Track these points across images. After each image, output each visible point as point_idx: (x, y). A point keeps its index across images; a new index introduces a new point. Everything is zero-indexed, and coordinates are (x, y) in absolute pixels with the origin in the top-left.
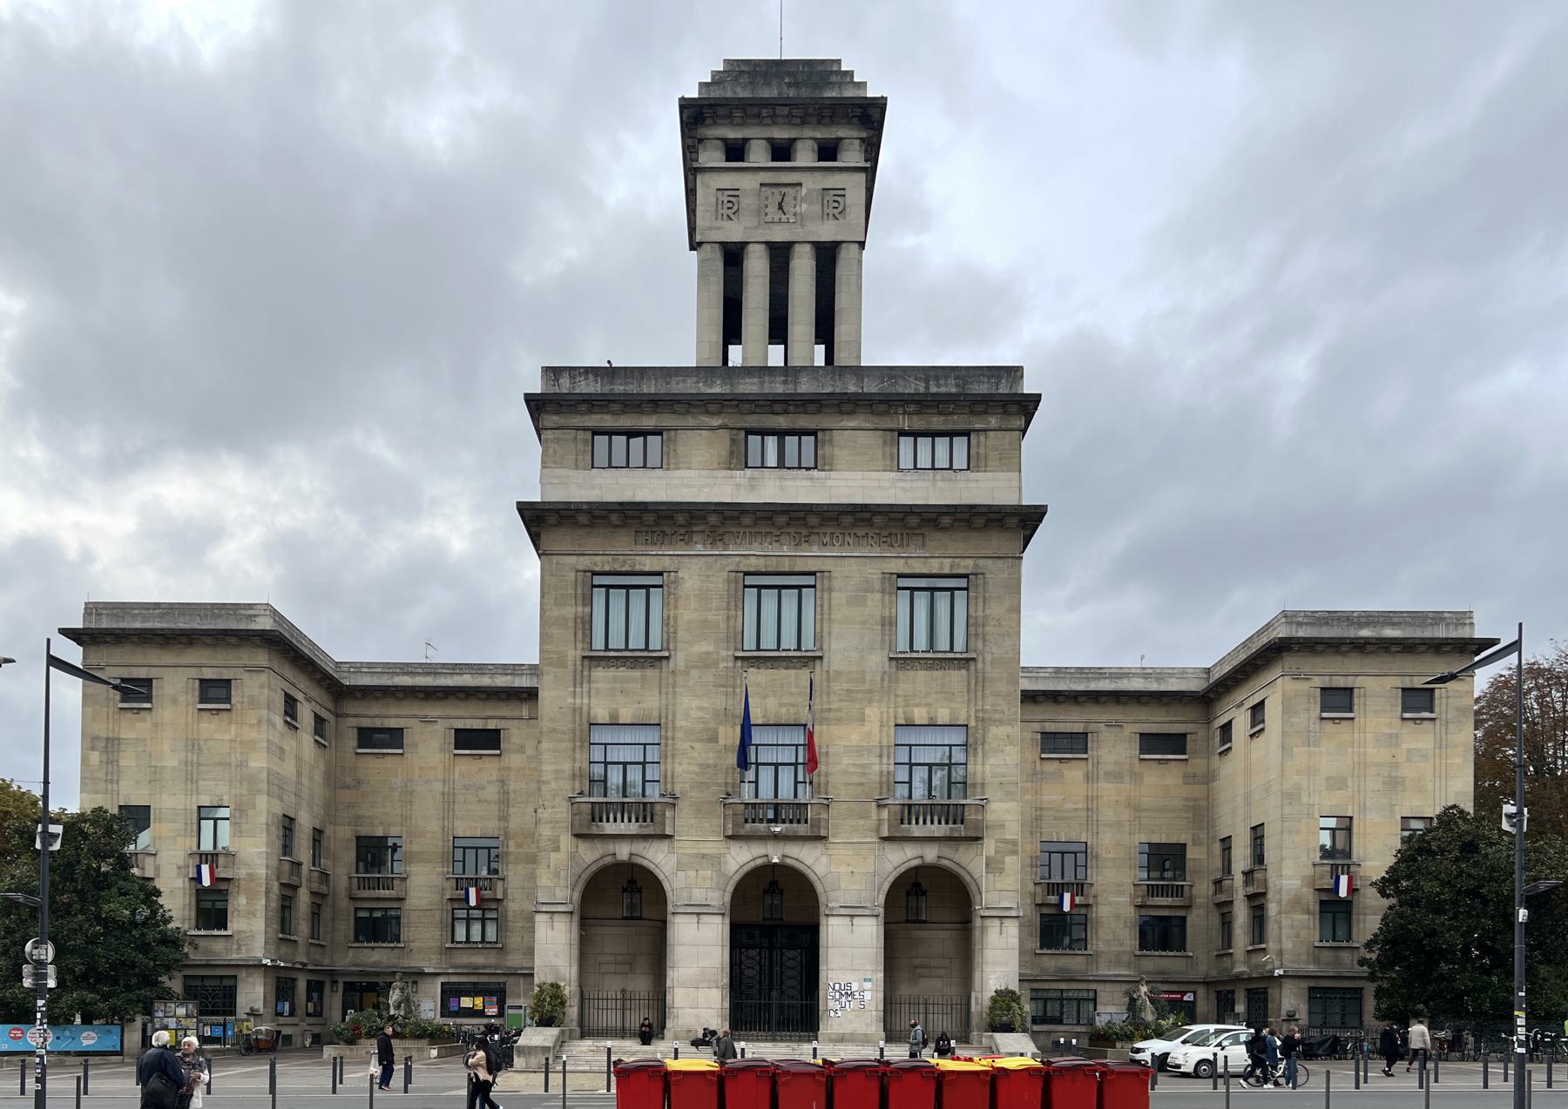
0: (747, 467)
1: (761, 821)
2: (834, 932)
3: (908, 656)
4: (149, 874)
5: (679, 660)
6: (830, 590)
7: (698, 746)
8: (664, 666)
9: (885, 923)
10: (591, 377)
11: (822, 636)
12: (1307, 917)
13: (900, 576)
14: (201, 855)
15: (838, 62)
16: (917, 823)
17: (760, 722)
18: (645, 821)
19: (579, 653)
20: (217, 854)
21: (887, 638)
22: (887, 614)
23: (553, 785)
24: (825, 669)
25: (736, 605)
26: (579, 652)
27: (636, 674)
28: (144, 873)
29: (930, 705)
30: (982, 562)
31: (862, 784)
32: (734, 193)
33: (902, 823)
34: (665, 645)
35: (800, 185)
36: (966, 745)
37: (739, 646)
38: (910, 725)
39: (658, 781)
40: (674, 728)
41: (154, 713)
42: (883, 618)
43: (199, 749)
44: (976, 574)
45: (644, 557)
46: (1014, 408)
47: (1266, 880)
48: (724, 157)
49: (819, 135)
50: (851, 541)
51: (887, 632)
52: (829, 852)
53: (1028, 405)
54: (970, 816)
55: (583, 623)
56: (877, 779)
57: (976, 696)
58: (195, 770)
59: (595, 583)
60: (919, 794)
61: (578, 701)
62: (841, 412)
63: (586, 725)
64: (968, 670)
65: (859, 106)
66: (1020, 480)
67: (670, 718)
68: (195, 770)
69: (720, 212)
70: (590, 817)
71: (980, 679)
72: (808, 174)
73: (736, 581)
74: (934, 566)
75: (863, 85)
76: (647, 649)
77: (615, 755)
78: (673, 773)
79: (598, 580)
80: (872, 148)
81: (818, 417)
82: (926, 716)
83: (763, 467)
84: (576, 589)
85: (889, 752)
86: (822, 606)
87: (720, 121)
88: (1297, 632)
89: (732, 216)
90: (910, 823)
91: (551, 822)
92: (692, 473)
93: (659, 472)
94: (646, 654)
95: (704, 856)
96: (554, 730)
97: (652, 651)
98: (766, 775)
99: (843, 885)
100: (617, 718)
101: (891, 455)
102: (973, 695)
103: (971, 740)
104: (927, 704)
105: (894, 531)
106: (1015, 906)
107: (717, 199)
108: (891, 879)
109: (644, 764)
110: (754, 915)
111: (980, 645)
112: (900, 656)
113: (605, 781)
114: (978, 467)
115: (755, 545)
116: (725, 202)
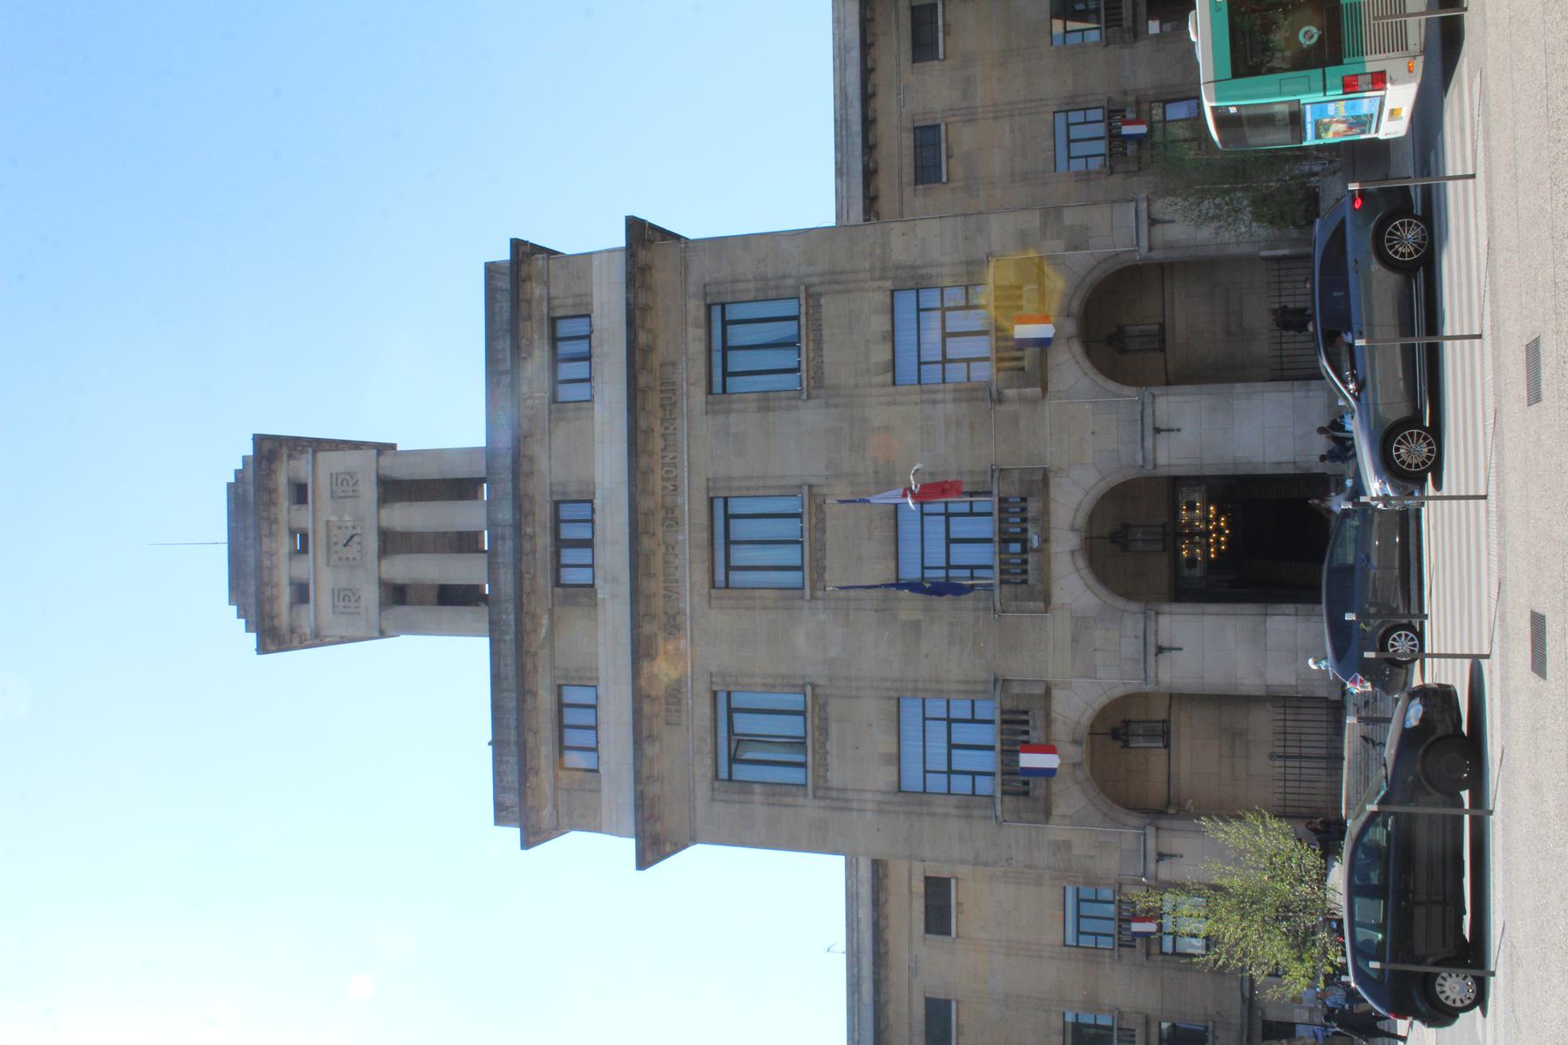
0: (592, 586)
1: (1025, 562)
3: (804, 375)
6: (729, 479)
9: (1168, 383)
11: (785, 487)
13: (710, 391)
17: (892, 564)
18: (1026, 722)
21: (784, 403)
27: (834, 728)
30: (692, 289)
31: (972, 426)
34: (797, 690)
35: (328, 522)
37: (798, 593)
38: (893, 366)
39: (973, 701)
44: (706, 295)
46: (525, 270)
48: (306, 605)
49: (286, 504)
61: (869, 806)
62: (531, 474)
63: (900, 797)
64: (820, 295)
65: (260, 463)
66: (600, 252)
74: (697, 348)
75: (245, 458)
76: (802, 713)
77: (938, 759)
78: (960, 682)
83: (592, 566)
84: (735, 802)
86: (749, 488)
89: (356, 597)
93: (601, 690)
94: (809, 715)
95: (1075, 640)
98: (961, 554)
103: (911, 284)
108: (1100, 379)
109: (950, 721)
111: (790, 282)
114: (587, 304)
116: (344, 604)
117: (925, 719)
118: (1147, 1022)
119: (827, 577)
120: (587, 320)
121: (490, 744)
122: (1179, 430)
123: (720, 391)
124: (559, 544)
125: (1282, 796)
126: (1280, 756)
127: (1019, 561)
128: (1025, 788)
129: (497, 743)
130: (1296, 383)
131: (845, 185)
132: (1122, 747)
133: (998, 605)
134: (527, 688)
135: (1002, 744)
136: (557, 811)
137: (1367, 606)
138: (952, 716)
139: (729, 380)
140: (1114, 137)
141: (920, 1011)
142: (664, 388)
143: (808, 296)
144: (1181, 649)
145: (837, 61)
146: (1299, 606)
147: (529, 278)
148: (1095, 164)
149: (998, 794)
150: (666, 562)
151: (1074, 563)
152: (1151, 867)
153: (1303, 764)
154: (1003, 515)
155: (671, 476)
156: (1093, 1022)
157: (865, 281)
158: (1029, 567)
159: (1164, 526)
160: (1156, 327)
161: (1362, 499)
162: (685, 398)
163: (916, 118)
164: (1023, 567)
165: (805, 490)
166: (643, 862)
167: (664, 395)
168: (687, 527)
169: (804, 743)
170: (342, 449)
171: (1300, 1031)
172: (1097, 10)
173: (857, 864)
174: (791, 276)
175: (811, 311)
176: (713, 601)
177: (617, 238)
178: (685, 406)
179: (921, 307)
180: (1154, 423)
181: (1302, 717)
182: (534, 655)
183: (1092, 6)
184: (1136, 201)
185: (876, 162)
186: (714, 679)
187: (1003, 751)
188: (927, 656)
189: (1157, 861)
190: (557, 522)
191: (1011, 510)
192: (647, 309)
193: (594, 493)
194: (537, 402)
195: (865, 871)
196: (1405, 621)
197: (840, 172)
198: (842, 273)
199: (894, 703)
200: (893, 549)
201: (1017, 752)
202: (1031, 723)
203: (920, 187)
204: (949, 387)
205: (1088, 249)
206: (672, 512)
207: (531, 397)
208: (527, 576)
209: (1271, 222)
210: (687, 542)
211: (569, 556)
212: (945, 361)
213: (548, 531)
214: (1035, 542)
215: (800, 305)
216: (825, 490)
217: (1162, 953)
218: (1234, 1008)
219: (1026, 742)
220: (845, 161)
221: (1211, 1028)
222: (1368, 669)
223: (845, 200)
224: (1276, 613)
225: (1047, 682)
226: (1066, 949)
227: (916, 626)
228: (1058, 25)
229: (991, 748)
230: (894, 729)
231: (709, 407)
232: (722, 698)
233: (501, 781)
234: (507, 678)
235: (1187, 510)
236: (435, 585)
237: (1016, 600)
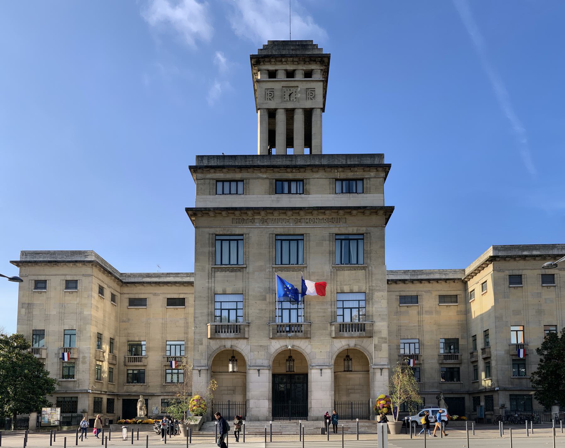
0: (276, 193)
1: (284, 332)
2: (314, 375)
3: (339, 266)
4: (44, 356)
5: (250, 269)
6: (309, 241)
7: (258, 302)
8: (244, 271)
10: (216, 159)
11: (306, 259)
12: (507, 366)
13: (336, 234)
14: (65, 349)
15: (312, 41)
16: (346, 331)
18: (237, 332)
19: (211, 266)
20: (71, 349)
21: (331, 259)
22: (331, 250)
23: (200, 318)
24: (308, 271)
25: (273, 247)
26: (210, 266)
28: (41, 356)
29: (350, 285)
30: (369, 229)
31: (324, 316)
32: (272, 90)
33: (340, 331)
34: (245, 262)
35: (298, 87)
38: (343, 292)
40: (248, 295)
41: (47, 293)
42: (330, 251)
43: (65, 307)
44: (367, 233)
45: (236, 228)
46: (380, 169)
47: (490, 352)
49: (304, 68)
51: (331, 257)
52: (312, 343)
53: (388, 167)
54: (367, 328)
56: (330, 314)
57: (369, 281)
58: (63, 315)
59: (217, 239)
60: (347, 320)
62: (313, 172)
63: (213, 294)
64: (365, 270)
65: (319, 57)
66: (384, 197)
67: (247, 291)
68: (63, 315)
69: (267, 97)
70: (215, 331)
71: (370, 274)
72: (300, 83)
73: (272, 238)
74: (350, 230)
76: (237, 264)
77: (225, 306)
78: (248, 313)
79: (218, 238)
80: (326, 73)
81: (305, 174)
82: (349, 289)
84: (209, 241)
86: (306, 247)
87: (266, 63)
88: (498, 253)
90: (343, 331)
91: (199, 334)
92: (255, 196)
93: (242, 196)
94: (237, 266)
95: (261, 346)
96: (200, 296)
99: (317, 357)
100: (226, 291)
101: (333, 188)
102: (368, 280)
103: (367, 298)
104: (349, 284)
105: (334, 217)
106: (387, 364)
107: (265, 92)
108: (336, 354)
109: (236, 309)
110: (282, 370)
112: (337, 266)
113: (221, 316)
114: (367, 192)
116: (269, 93)
119: (279, 272)
125: (218, 404)
127: (284, 330)
128: (218, 332)
129: (224, 157)
138: (238, 310)
146: (271, 409)
153: (227, 410)
157: (369, 284)
159: (294, 371)
160: (351, 370)
162: (334, 226)
164: (282, 331)
165: (305, 266)
167: (336, 219)
168: (295, 227)
170: (323, 91)
176: (271, 235)
178: (332, 226)
180: (323, 369)
181: (240, 409)
184: (388, 365)
186: (247, 235)
188: (256, 303)
190: (297, 181)
192: (363, 213)
194: (336, 174)
198: (372, 277)
199: (241, 293)
204: (336, 310)
211: (286, 185)
213: (293, 178)
214: (290, 335)
216: (305, 271)
225: (249, 338)
227: (265, 299)
230: (233, 293)
231: (331, 234)
237: (272, 329)
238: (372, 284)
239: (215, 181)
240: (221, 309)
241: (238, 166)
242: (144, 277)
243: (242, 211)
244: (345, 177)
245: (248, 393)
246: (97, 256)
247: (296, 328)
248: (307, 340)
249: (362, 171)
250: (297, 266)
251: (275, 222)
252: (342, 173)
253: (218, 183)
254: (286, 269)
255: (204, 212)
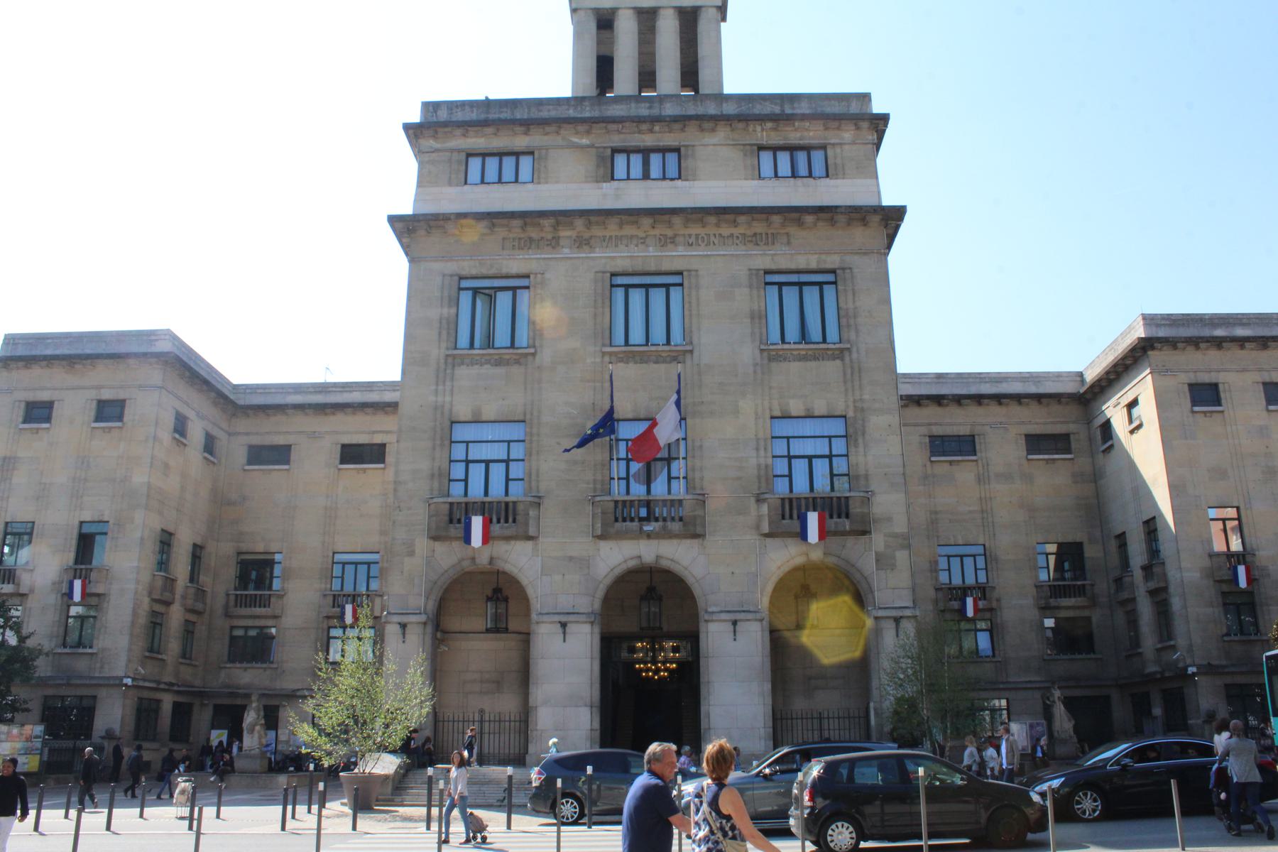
0: (613, 179)
1: (632, 520)
3: (779, 347)
5: (545, 356)
6: (698, 287)
11: (691, 332)
13: (767, 272)
17: (630, 416)
18: (507, 521)
22: (756, 307)
25: (603, 303)
27: (500, 371)
30: (848, 258)
31: (739, 478)
33: (783, 518)
34: (531, 341)
36: (846, 436)
37: (607, 342)
38: (786, 416)
39: (522, 480)
44: (843, 269)
50: (716, 242)
53: (880, 123)
54: (855, 509)
55: (448, 323)
57: (853, 386)
60: (801, 486)
61: (440, 399)
62: (702, 130)
64: (842, 359)
66: (878, 185)
67: (535, 414)
70: (447, 518)
74: (801, 262)
76: (513, 346)
77: (477, 452)
78: (538, 471)
79: (464, 284)
83: (628, 178)
84: (442, 292)
85: (766, 445)
86: (690, 303)
93: (530, 186)
94: (511, 351)
95: (571, 559)
97: (518, 348)
103: (851, 430)
105: (758, 230)
111: (853, 336)
112: (771, 347)
115: (622, 247)
117: (509, 442)
118: (275, 617)
120: (825, 175)
121: (487, 97)
122: (735, 640)
123: (767, 280)
124: (646, 152)
125: (451, 719)
126: (482, 718)
127: (633, 515)
128: (455, 521)
129: (487, 104)
130: (771, 730)
131: (929, 380)
132: (487, 596)
133: (598, 499)
134: (532, 127)
135: (490, 503)
136: (433, 152)
137: (598, 783)
139: (776, 288)
140: (964, 591)
141: (280, 440)
142: (770, 236)
143: (842, 350)
144: (564, 641)
145: (1027, 375)
146: (599, 732)
147: (858, 128)
148: (944, 578)
149: (450, 500)
150: (632, 237)
151: (632, 559)
152: (396, 619)
154: (669, 503)
155: (700, 241)
156: (275, 575)
157: (853, 394)
158: (628, 523)
161: (679, 778)
162: (761, 252)
163: (982, 437)
164: (628, 519)
165: (689, 348)
166: (394, 220)
167: (764, 236)
168: (660, 254)
169: (489, 347)
171: (272, 734)
172: (1064, 579)
173: (394, 390)
174: (857, 336)
175: (829, 353)
176: (600, 275)
177: (889, 199)
178: (755, 252)
179: (833, 439)
180: (741, 620)
181: (512, 736)
182: (558, 133)
183: (1068, 575)
184: (914, 608)
185: (947, 405)
186: (539, 276)
187: (484, 503)
189: (400, 624)
190: (664, 151)
191: (673, 509)
192: (832, 222)
193: (687, 180)
194: (759, 135)
195: (389, 397)
196: (586, 812)
197: (940, 377)
198: (860, 377)
199: (521, 418)
200: (642, 417)
201: (483, 514)
202: (506, 525)
203: (927, 440)
205: (877, 569)
206: (671, 242)
207: (763, 130)
208: (621, 126)
209: (896, 713)
210: (648, 254)
211: (636, 160)
212: (790, 458)
214: (648, 528)
215: (835, 344)
217: (329, 628)
218: (288, 684)
219: (491, 521)
220: (949, 381)
221: (272, 666)
222: (548, 783)
223: (917, 380)
224: (594, 715)
226: (331, 554)
228: (1052, 548)
229: (486, 493)
230: (500, 419)
231: (754, 272)
232: (524, 282)
233: (457, 107)
234: (541, 111)
235: (673, 646)
236: (612, 52)
238: (861, 395)
239: (463, 156)
240: (468, 462)
241: (519, 120)
242: (289, 393)
243: (528, 220)
244: (781, 142)
245: (532, 689)
246: (175, 338)
247: (665, 509)
248: (695, 542)
249: (822, 128)
250: (667, 348)
251: (610, 245)
252: (773, 134)
253: (471, 159)
254: (638, 358)
255: (432, 223)
